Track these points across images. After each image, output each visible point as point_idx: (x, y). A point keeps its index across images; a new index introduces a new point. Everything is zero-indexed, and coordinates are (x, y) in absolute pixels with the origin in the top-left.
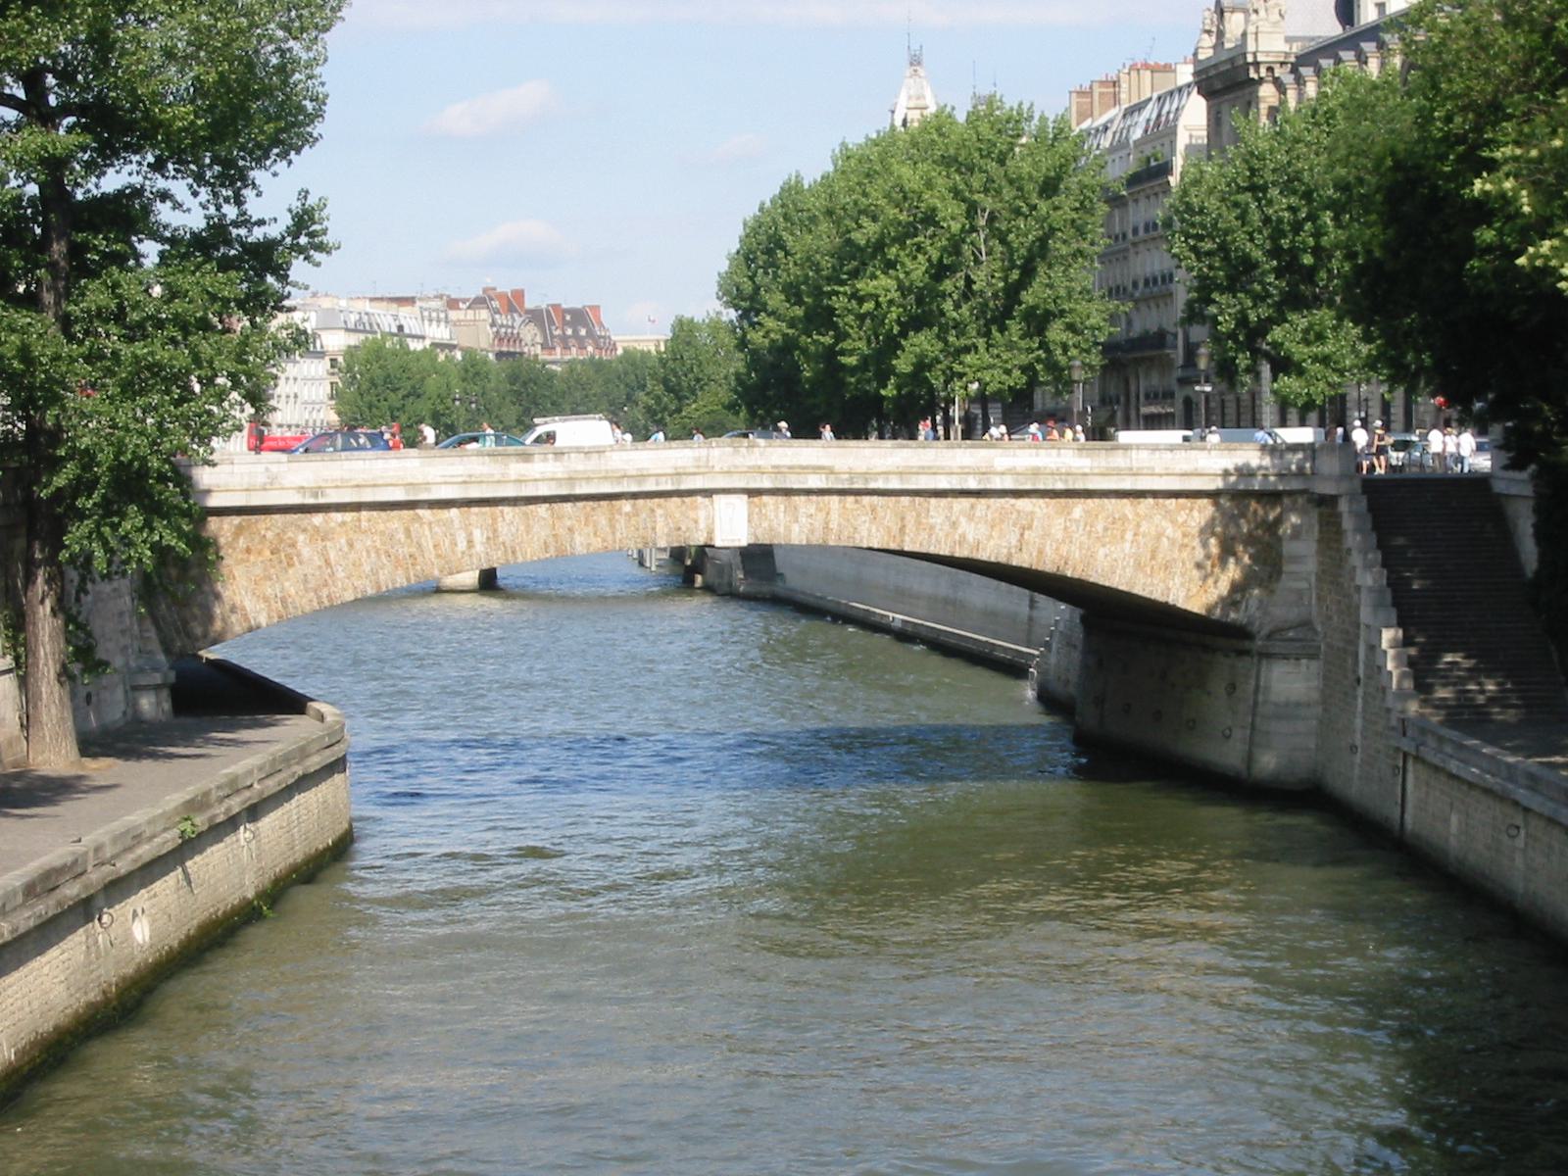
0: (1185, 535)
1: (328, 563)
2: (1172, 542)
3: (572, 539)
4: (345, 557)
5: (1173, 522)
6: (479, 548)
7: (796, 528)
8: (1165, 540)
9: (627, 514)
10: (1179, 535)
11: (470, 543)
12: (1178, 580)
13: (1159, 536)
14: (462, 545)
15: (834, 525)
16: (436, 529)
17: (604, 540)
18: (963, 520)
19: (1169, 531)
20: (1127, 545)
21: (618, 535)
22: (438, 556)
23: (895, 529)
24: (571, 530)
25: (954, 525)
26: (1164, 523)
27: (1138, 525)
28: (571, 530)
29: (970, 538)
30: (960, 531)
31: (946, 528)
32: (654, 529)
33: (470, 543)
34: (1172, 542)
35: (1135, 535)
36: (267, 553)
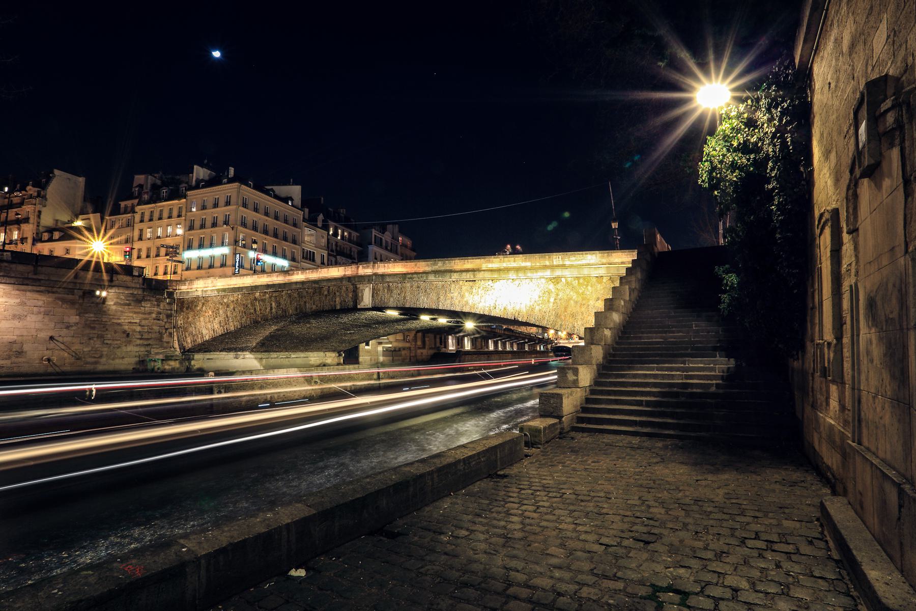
0: (583, 299)
1: (227, 317)
2: (576, 302)
3: (305, 305)
4: (232, 314)
5: (577, 293)
6: (274, 310)
7: (392, 299)
8: (572, 302)
9: (326, 295)
10: (580, 299)
11: (271, 309)
12: (579, 323)
13: (570, 299)
14: (268, 310)
15: (408, 298)
16: (261, 303)
17: (317, 306)
18: (467, 294)
19: (575, 297)
20: (551, 304)
21: (322, 304)
22: (261, 313)
23: (435, 298)
24: (305, 302)
25: (462, 297)
26: (572, 293)
27: (557, 295)
28: (305, 302)
29: (470, 302)
30: (465, 299)
31: (459, 298)
32: (335, 301)
33: (271, 309)
34: (576, 302)
35: (555, 299)
36: (210, 313)
